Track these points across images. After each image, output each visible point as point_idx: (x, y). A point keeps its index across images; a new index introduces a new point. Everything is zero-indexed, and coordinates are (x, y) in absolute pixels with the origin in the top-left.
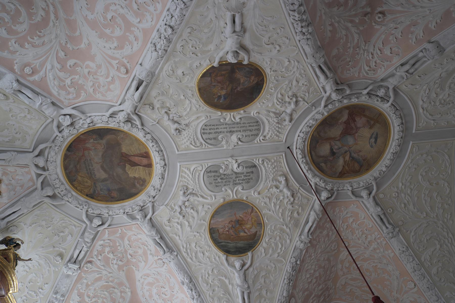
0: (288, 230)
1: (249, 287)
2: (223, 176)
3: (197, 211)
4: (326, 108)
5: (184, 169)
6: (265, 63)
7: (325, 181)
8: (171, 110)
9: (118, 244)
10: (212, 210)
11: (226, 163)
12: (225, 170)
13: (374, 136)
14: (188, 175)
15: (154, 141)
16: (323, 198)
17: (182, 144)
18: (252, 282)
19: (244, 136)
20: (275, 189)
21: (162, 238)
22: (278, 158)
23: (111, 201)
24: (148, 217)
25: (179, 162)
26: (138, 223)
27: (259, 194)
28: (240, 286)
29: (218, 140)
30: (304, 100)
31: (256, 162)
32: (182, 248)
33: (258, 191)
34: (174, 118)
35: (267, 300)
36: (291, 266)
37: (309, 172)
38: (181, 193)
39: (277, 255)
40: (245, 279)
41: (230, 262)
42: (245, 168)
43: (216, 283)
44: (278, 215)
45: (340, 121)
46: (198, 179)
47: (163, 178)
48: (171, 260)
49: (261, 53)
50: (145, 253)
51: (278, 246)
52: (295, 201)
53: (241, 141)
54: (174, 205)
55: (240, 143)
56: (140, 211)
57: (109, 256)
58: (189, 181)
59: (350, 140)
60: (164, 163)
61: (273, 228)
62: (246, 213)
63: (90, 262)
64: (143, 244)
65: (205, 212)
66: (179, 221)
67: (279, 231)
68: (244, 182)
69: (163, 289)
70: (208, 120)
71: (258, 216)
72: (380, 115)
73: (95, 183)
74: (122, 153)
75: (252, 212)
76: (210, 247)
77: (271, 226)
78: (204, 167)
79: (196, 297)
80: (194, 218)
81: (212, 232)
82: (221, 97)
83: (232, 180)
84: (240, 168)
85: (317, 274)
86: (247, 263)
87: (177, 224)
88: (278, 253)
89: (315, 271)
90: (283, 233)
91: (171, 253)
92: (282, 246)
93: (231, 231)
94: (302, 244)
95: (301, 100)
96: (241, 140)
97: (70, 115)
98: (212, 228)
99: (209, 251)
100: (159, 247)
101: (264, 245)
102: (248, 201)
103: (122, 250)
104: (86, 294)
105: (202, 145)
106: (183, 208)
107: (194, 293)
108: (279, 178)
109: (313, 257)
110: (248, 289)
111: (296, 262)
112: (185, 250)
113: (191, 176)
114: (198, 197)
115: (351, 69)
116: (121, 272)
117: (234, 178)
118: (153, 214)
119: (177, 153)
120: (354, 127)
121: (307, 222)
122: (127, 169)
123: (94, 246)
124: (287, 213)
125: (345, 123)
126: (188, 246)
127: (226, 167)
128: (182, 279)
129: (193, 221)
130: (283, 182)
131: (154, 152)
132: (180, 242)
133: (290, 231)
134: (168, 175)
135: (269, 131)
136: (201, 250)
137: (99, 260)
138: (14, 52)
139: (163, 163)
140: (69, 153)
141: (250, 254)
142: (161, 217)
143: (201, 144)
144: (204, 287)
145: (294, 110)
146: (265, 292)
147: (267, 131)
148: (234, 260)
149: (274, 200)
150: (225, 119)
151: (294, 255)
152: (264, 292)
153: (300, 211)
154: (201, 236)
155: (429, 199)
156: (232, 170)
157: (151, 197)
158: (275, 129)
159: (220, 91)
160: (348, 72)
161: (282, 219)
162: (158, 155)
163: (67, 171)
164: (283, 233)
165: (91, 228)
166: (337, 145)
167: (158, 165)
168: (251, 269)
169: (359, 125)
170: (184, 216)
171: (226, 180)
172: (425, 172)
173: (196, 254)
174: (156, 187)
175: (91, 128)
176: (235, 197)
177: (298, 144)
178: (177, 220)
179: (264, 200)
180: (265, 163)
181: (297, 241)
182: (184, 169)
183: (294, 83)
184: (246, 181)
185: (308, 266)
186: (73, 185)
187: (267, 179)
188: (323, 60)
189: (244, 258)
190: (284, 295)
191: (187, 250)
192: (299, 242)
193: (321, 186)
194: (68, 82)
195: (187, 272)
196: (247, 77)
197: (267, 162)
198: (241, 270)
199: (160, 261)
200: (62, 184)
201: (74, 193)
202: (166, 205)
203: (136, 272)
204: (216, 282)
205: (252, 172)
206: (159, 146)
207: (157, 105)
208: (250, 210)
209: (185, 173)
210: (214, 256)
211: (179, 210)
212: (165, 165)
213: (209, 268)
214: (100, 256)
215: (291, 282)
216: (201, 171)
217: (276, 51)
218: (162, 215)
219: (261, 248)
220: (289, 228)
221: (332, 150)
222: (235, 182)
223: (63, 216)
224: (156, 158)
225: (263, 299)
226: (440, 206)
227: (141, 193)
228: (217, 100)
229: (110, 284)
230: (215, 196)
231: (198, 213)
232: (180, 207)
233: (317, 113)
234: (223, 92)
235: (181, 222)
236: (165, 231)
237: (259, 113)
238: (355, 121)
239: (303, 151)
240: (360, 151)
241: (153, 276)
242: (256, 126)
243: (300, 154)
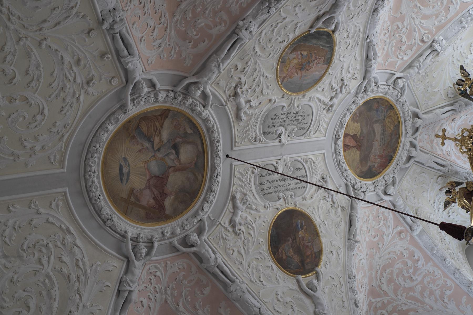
4: (199, 219)
6: (281, 277)
7: (193, 110)
8: (330, 206)
9: (393, 48)
11: (289, 139)
12: (293, 130)
13: (125, 177)
15: (340, 167)
23: (380, 99)
27: (270, 100)
29: (293, 167)
30: (226, 229)
31: (263, 138)
34: (327, 196)
37: (211, 126)
38: (334, 108)
39: (287, 20)
45: (172, 197)
49: (290, 289)
53: (274, 165)
55: (276, 165)
57: (406, 40)
59: (155, 168)
61: (271, 55)
62: (290, 77)
63: (422, 41)
68: (280, 116)
70: (304, 196)
72: (126, 213)
73: (384, 120)
74: (360, 150)
75: (284, 78)
81: (329, 61)
82: (300, 226)
83: (290, 118)
90: (263, 46)
91: (371, 42)
92: (273, 30)
95: (229, 228)
97: (386, 193)
98: (327, 64)
103: (393, 40)
104: (443, 8)
106: (339, 90)
115: (178, 270)
116: (404, 12)
120: (154, 189)
122: (360, 132)
123: (411, 57)
125: (166, 195)
133: (254, 48)
137: (415, 39)
138: (408, 249)
140: (392, 154)
141: (313, 31)
143: (306, 162)
145: (234, 213)
147: (252, 180)
150: (291, 197)
151: (268, 15)
153: (233, 70)
154: (340, 56)
155: (30, 72)
158: (246, 185)
159: (303, 235)
160: (181, 267)
163: (397, 136)
164: (263, 46)
165: (407, 79)
166: (171, 160)
169: (147, 192)
172: (36, 121)
175: (375, 179)
176: (293, 98)
178: (349, 75)
183: (242, 251)
184: (278, 117)
186: (399, 122)
188: (232, 288)
194: (381, 224)
196: (289, 257)
197: (253, 138)
200: (405, 126)
201: (401, 114)
203: (392, 7)
207: (339, 210)
208: (286, 80)
214: (413, 43)
217: (279, 293)
220: (254, 50)
221: (178, 153)
222: (288, 116)
223: (416, 92)
226: (9, 58)
228: (302, 223)
229: (418, 5)
231: (330, 83)
232: (341, 91)
233: (207, 212)
234: (301, 234)
237: (265, 207)
238: (154, 198)
240: (140, 151)
242: (264, 189)
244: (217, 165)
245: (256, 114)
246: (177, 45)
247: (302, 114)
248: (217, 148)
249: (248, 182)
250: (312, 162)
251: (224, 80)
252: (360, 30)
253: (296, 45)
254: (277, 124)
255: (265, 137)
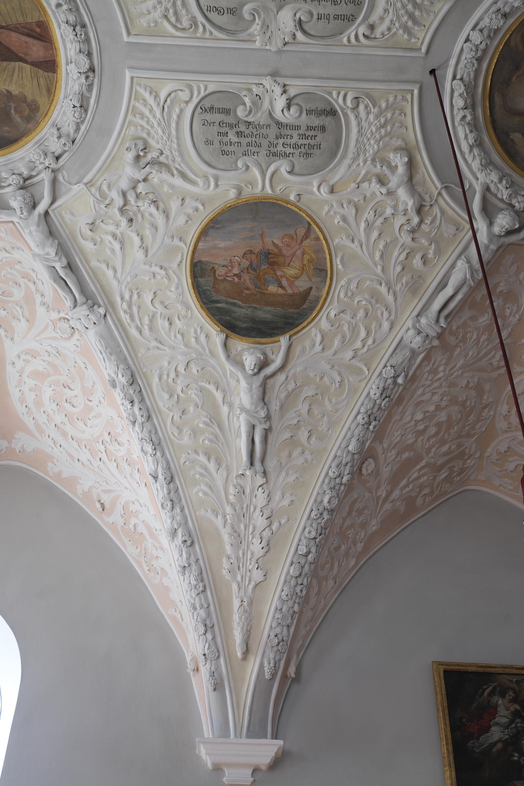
0: (390, 298)
1: (268, 417)
2: (242, 128)
3: (166, 213)
5: (141, 90)
7: (512, 185)
10: (205, 215)
11: (255, 90)
12: (250, 111)
14: (151, 110)
16: (496, 229)
17: (142, 14)
18: (277, 408)
19: (315, 17)
20: (375, 186)
21: (70, 267)
22: (399, 97)
24: (41, 208)
25: (131, 68)
26: (15, 220)
27: (332, 191)
28: (247, 412)
29: (241, 17)
32: (118, 299)
33: (332, 183)
35: (307, 452)
36: (381, 386)
37: (476, 151)
39: (349, 354)
40: (263, 397)
41: (233, 352)
42: (304, 113)
43: (193, 396)
44: (372, 255)
46: (177, 124)
47: (84, 107)
48: (91, 326)
50: (29, 299)
51: (359, 333)
52: (423, 226)
53: (304, 32)
54: (109, 187)
55: (300, 36)
56: (22, 188)
58: (152, 127)
60: (88, 62)
61: (353, 286)
62: (292, 238)
64: (25, 276)
65: (186, 218)
66: (118, 232)
67: (367, 296)
68: (297, 152)
69: (67, 390)
71: (319, 251)
75: (306, 236)
76: (188, 308)
77: (349, 282)
78: (196, 93)
79: (140, 420)
80: (156, 229)
81: (199, 271)
83: (265, 143)
84: (293, 109)
85: (442, 417)
86: (273, 361)
87: (110, 238)
88: (356, 351)
89: (438, 408)
90: (377, 302)
92: (368, 334)
93: (246, 277)
94: (418, 339)
96: (306, 27)
98: (200, 262)
99: (185, 317)
100: (63, 289)
101: (324, 324)
102: (299, 204)
105: (196, 25)
107: (136, 409)
108: (391, 156)
109: (441, 374)
110: (265, 422)
111: (395, 377)
112: (125, 306)
113: (158, 115)
114: (173, 175)
117: (272, 137)
118: (52, 203)
119: (126, 38)
121: (442, 285)
124: (396, 253)
126: (135, 297)
127: (254, 103)
128: (113, 375)
129: (154, 237)
130: (401, 170)
131: (64, 26)
132: (114, 283)
133: (396, 300)
134: (98, 101)
135: (386, 11)
136: (165, 311)
139: (85, 63)
141: (284, 340)
142: (72, 214)
143: (194, 23)
144: (162, 400)
146: (306, 434)
147: (379, 11)
148: (243, 350)
149: (368, 214)
151: (393, 362)
152: (303, 435)
154: (169, 278)
156: (270, 113)
157: (50, 155)
158: (404, 6)
161: (379, 268)
162: (72, 37)
164: (377, 302)
167: (72, 66)
168: (281, 377)
170: (131, 220)
171: (249, 140)
173: (151, 321)
174: (64, 130)
177: (461, 65)
178: (111, 228)
179: (341, 211)
180: (362, 107)
181: (408, 329)
182: (141, 90)
185: (423, 394)
187: (358, 155)
189: (268, 348)
190: (351, 448)
191: (130, 306)
192: (411, 332)
193: (499, 196)
195: (126, 359)
197: (366, 107)
198: (255, 374)
199: (65, 325)
202: (89, 184)
204: (193, 394)
205: (323, 129)
206: (78, 9)
208: (301, 232)
209: (145, 103)
210: (196, 332)
211: (119, 201)
212: (92, 69)
213: (179, 357)
215: (374, 423)
216: (187, 102)
218: (77, 207)
219: (314, 331)
220: (395, 294)
222: (273, 150)
224: (69, 45)
225: (299, 450)
227: (25, 140)
230: (217, 179)
231: (167, 217)
235: (122, 234)
236: (82, 251)
239: (470, 89)
241: (46, 358)
243: (461, 95)
244: (473, 65)
245: (365, 162)
246: (520, 282)
247: (231, 148)
248: (466, 102)
249: (396, 10)
250: (173, 19)
251: (446, 235)
252: (140, 332)
253: (305, 306)
254: (301, 132)
255: (330, 103)
